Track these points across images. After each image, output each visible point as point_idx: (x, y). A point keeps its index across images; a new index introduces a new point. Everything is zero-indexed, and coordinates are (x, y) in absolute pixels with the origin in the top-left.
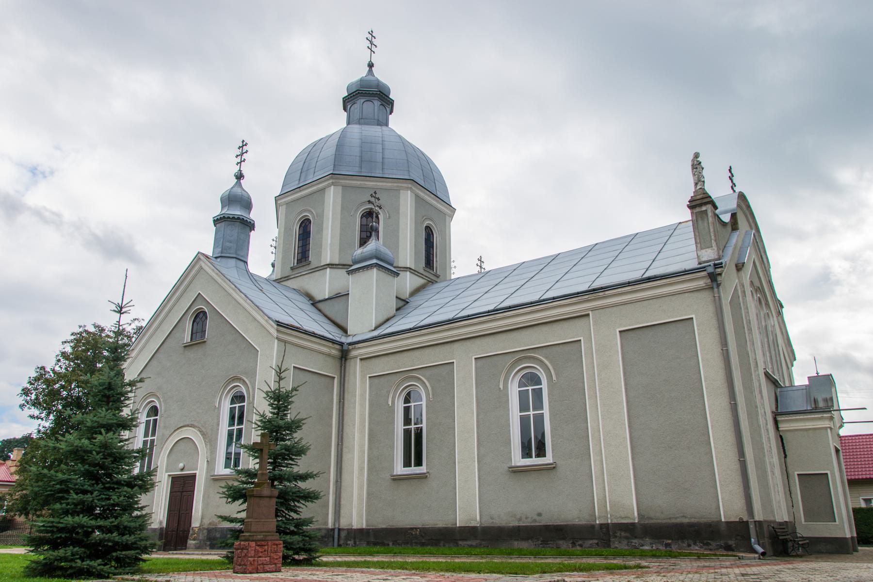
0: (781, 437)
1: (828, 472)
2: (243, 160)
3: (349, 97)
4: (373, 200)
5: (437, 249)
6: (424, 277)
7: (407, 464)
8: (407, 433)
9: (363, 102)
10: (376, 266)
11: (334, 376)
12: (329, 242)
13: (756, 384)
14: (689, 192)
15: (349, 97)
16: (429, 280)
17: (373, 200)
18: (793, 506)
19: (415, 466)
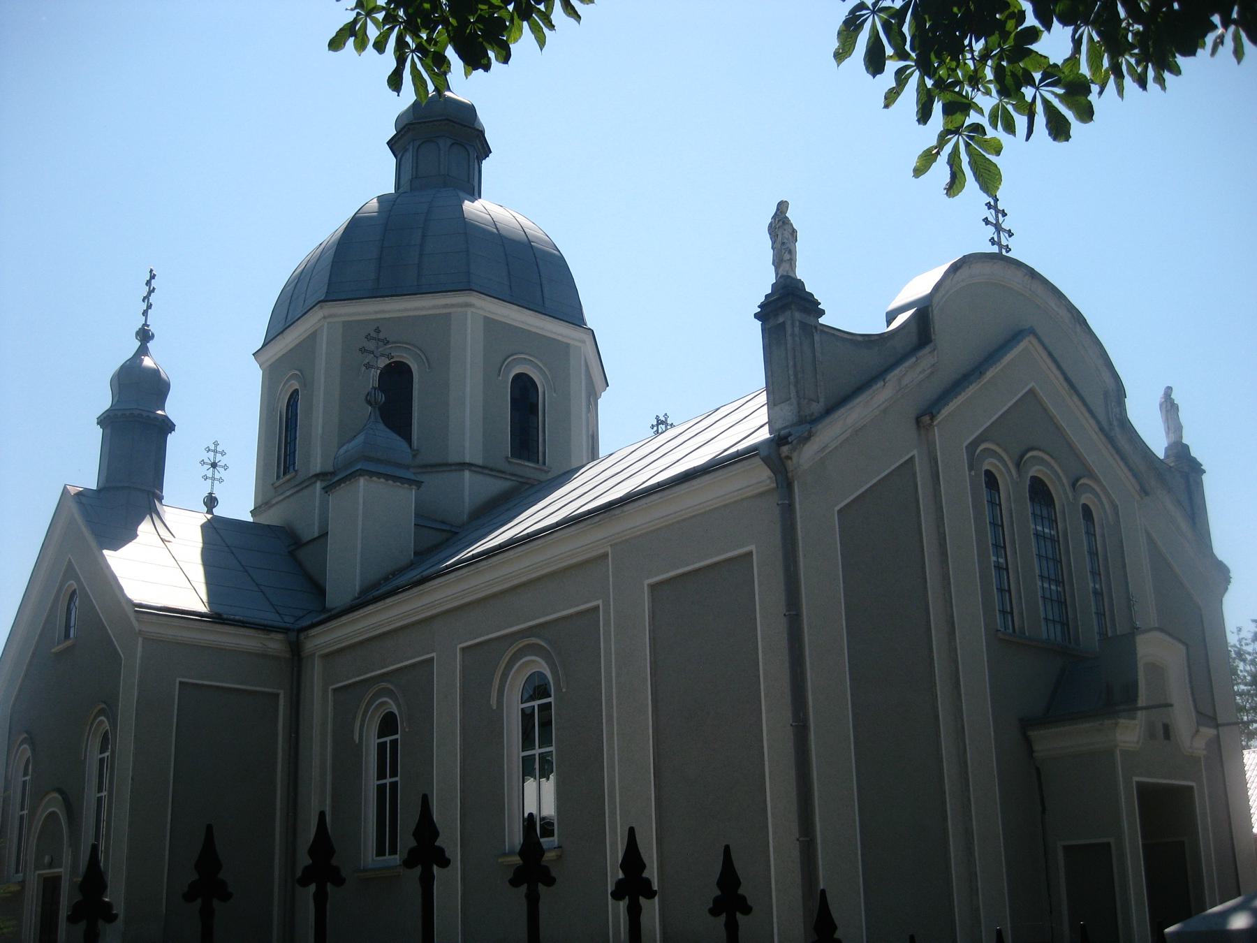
0: (1038, 769)
1: (1112, 840)
2: (146, 301)
3: (399, 136)
4: (371, 345)
5: (544, 416)
6: (497, 474)
7: (380, 852)
8: (381, 789)
9: (419, 146)
10: (360, 475)
11: (275, 691)
12: (320, 431)
13: (108, 775)
14: (764, 282)
15: (399, 136)
16: (520, 480)
17: (371, 345)
18: (1051, 912)
19: (390, 854)
